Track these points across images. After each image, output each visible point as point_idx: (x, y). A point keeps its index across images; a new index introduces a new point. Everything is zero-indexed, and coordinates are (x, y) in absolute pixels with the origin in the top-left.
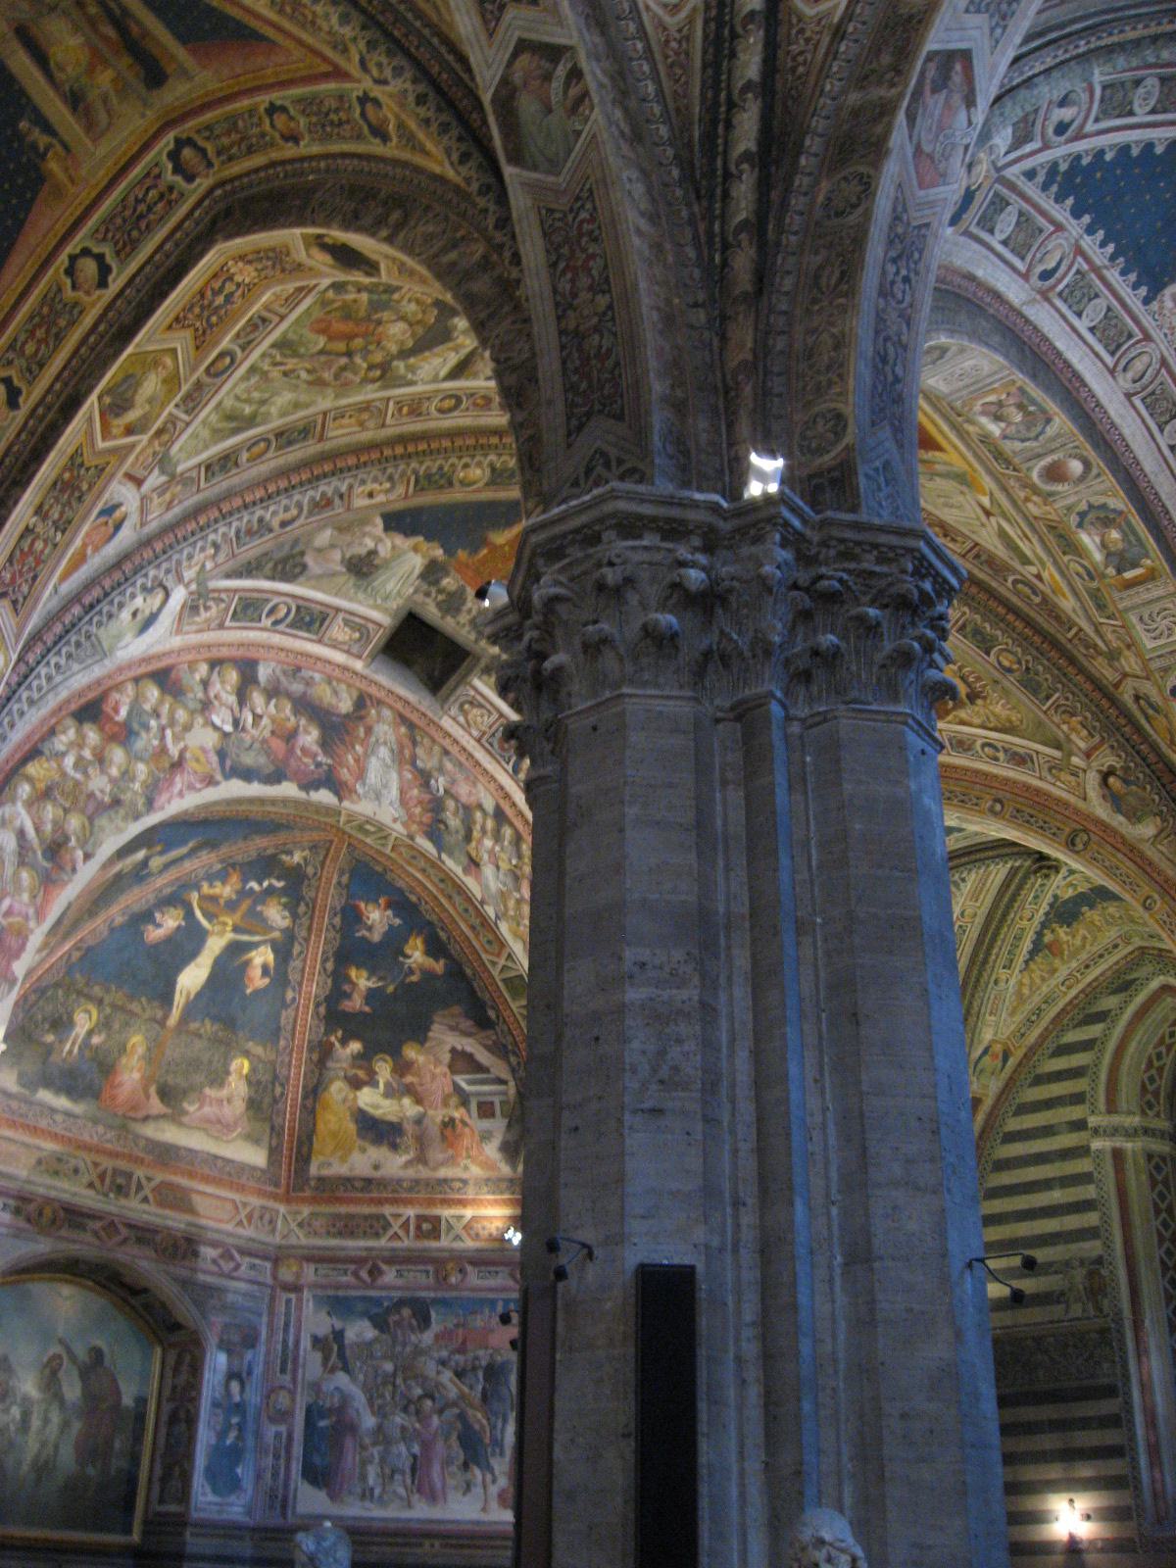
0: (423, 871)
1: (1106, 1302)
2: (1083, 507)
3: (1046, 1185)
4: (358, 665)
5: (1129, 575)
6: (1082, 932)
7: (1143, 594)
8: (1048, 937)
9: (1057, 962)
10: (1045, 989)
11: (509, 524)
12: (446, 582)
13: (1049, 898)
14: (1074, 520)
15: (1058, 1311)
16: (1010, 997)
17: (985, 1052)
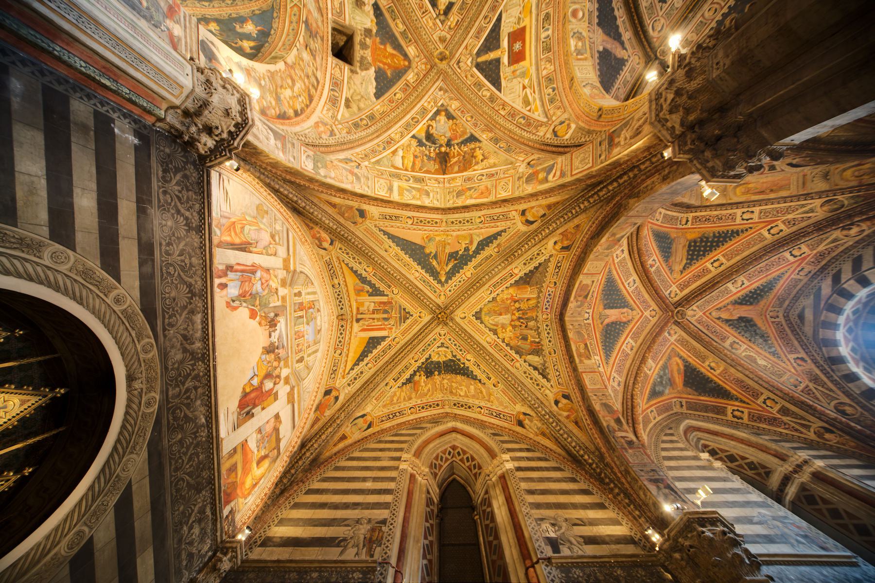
0: (291, 22)
1: (378, 549)
2: (576, 31)
3: (364, 479)
4: (330, 15)
5: (579, 57)
6: (430, 386)
7: (581, 63)
8: (417, 378)
9: (413, 395)
10: (402, 406)
11: (394, 49)
12: (367, 39)
13: (427, 356)
14: (572, 34)
15: (333, 554)
16: (386, 399)
17: (363, 416)
